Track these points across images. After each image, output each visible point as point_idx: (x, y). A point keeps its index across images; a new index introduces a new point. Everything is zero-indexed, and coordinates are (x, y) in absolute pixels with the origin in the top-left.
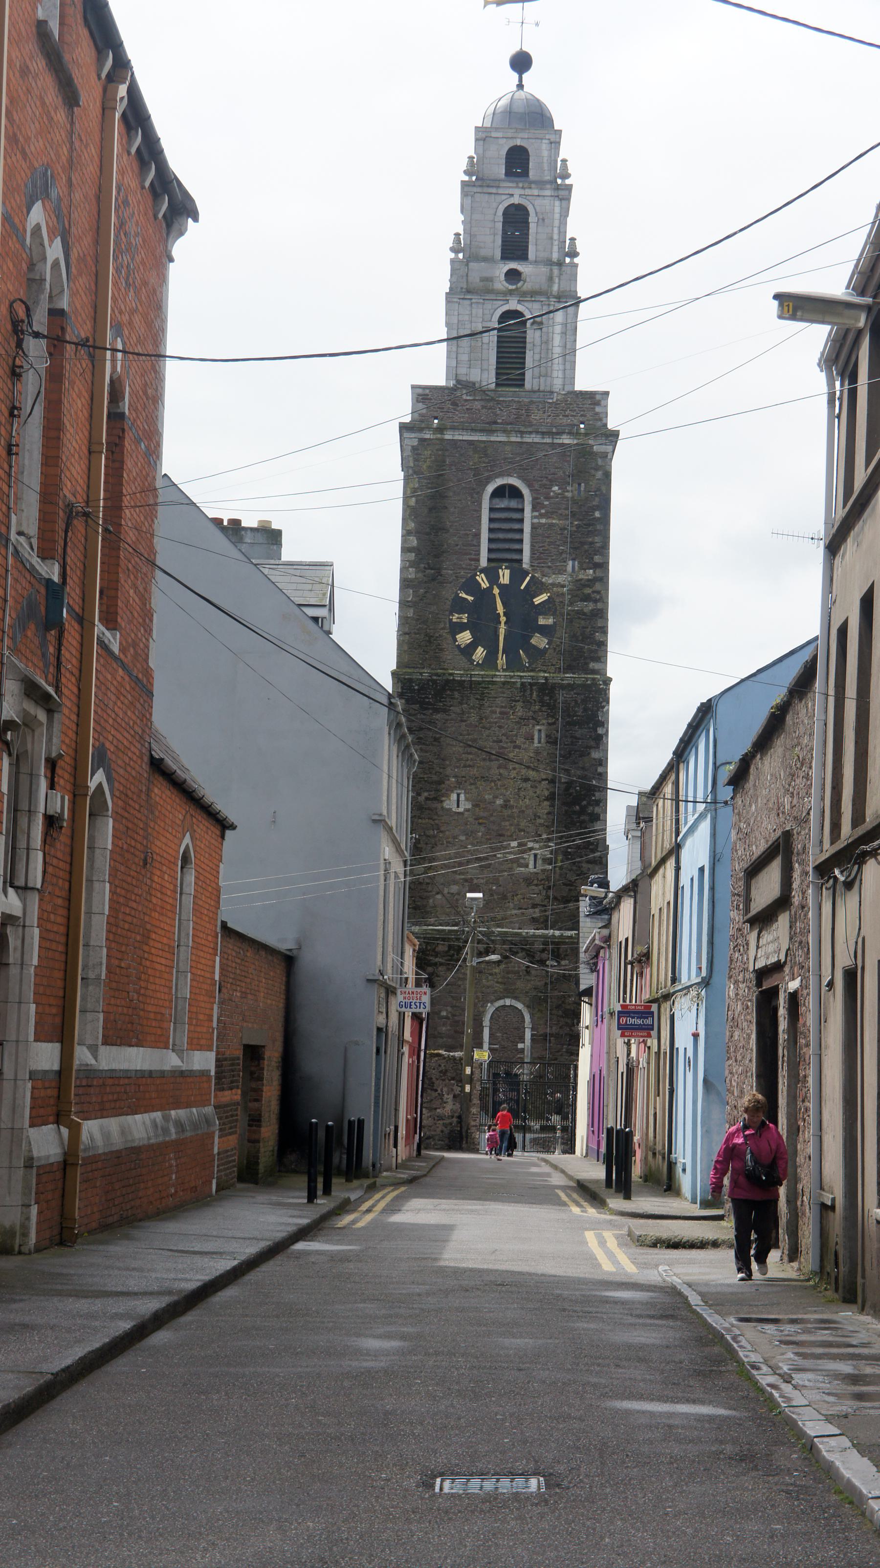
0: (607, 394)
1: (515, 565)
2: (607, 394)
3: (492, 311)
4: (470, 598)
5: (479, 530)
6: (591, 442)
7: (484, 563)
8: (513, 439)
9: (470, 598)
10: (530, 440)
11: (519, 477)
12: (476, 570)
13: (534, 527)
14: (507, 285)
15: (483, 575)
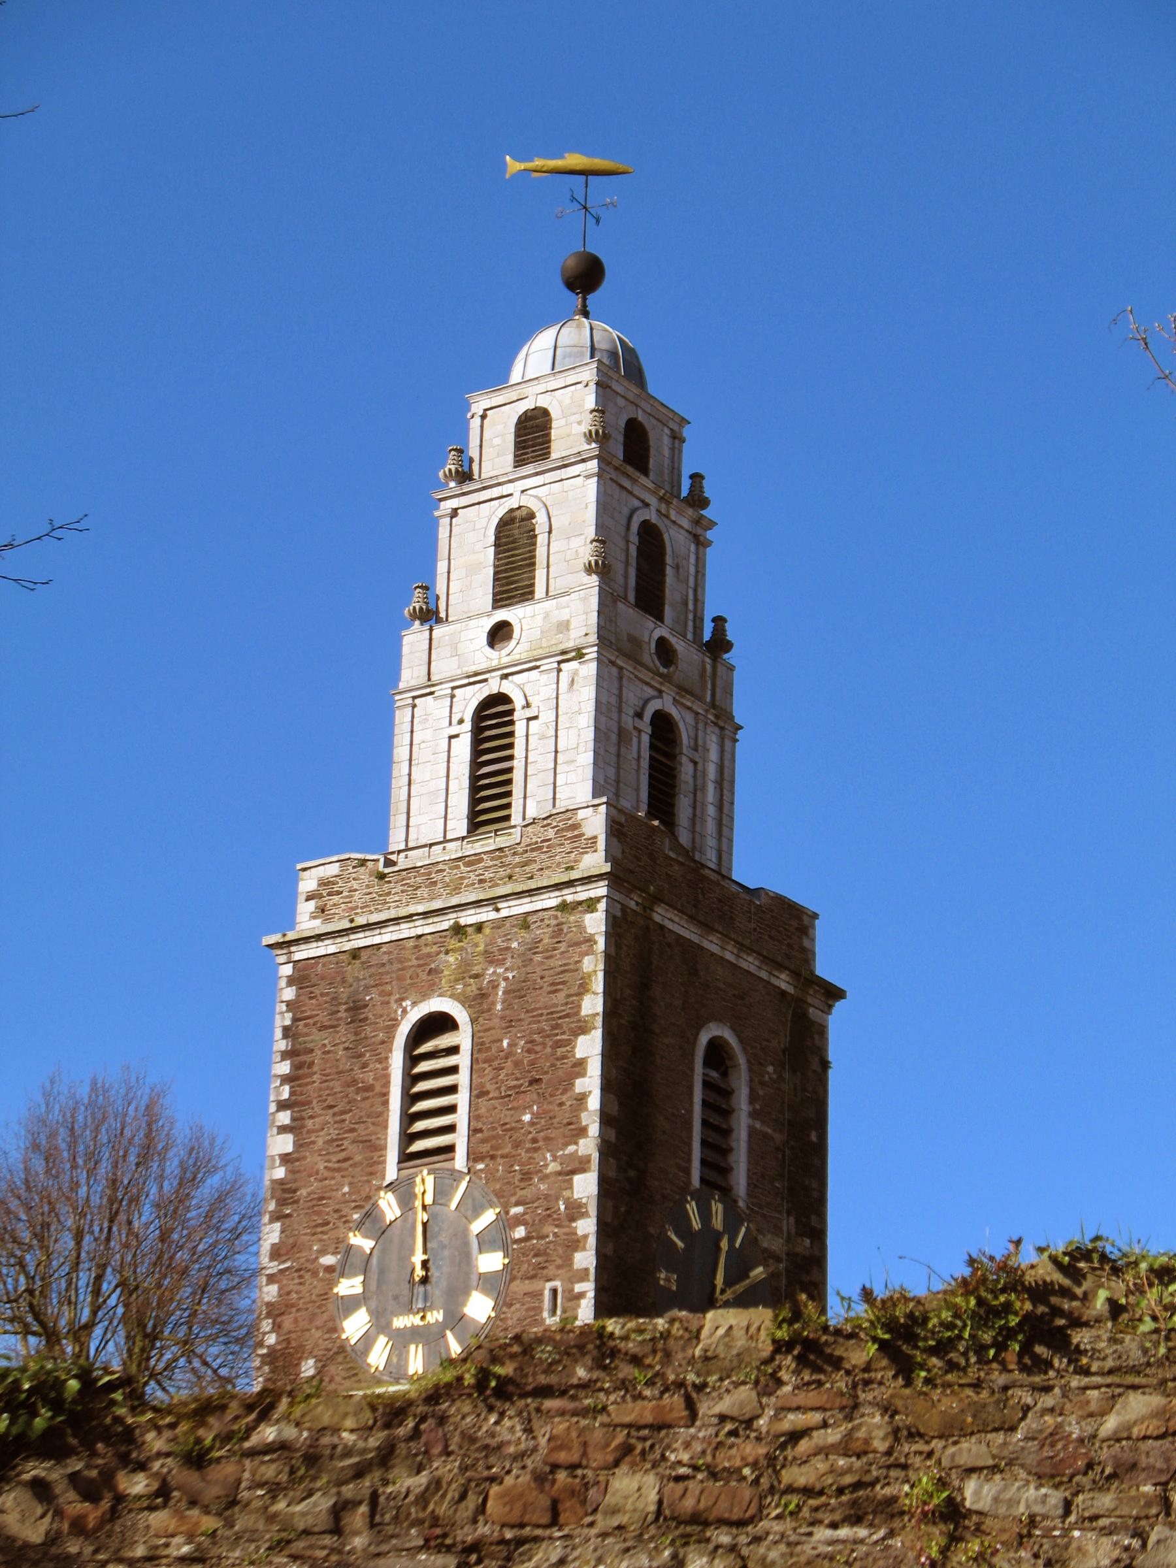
0: (815, 916)
1: (726, 1193)
2: (815, 916)
3: (641, 702)
4: (680, 1244)
5: (690, 1111)
6: (810, 1000)
7: (696, 1182)
8: (728, 956)
9: (680, 1244)
10: (744, 965)
11: (733, 1029)
12: (685, 1188)
13: (752, 1132)
14: (657, 662)
15: (693, 1203)
